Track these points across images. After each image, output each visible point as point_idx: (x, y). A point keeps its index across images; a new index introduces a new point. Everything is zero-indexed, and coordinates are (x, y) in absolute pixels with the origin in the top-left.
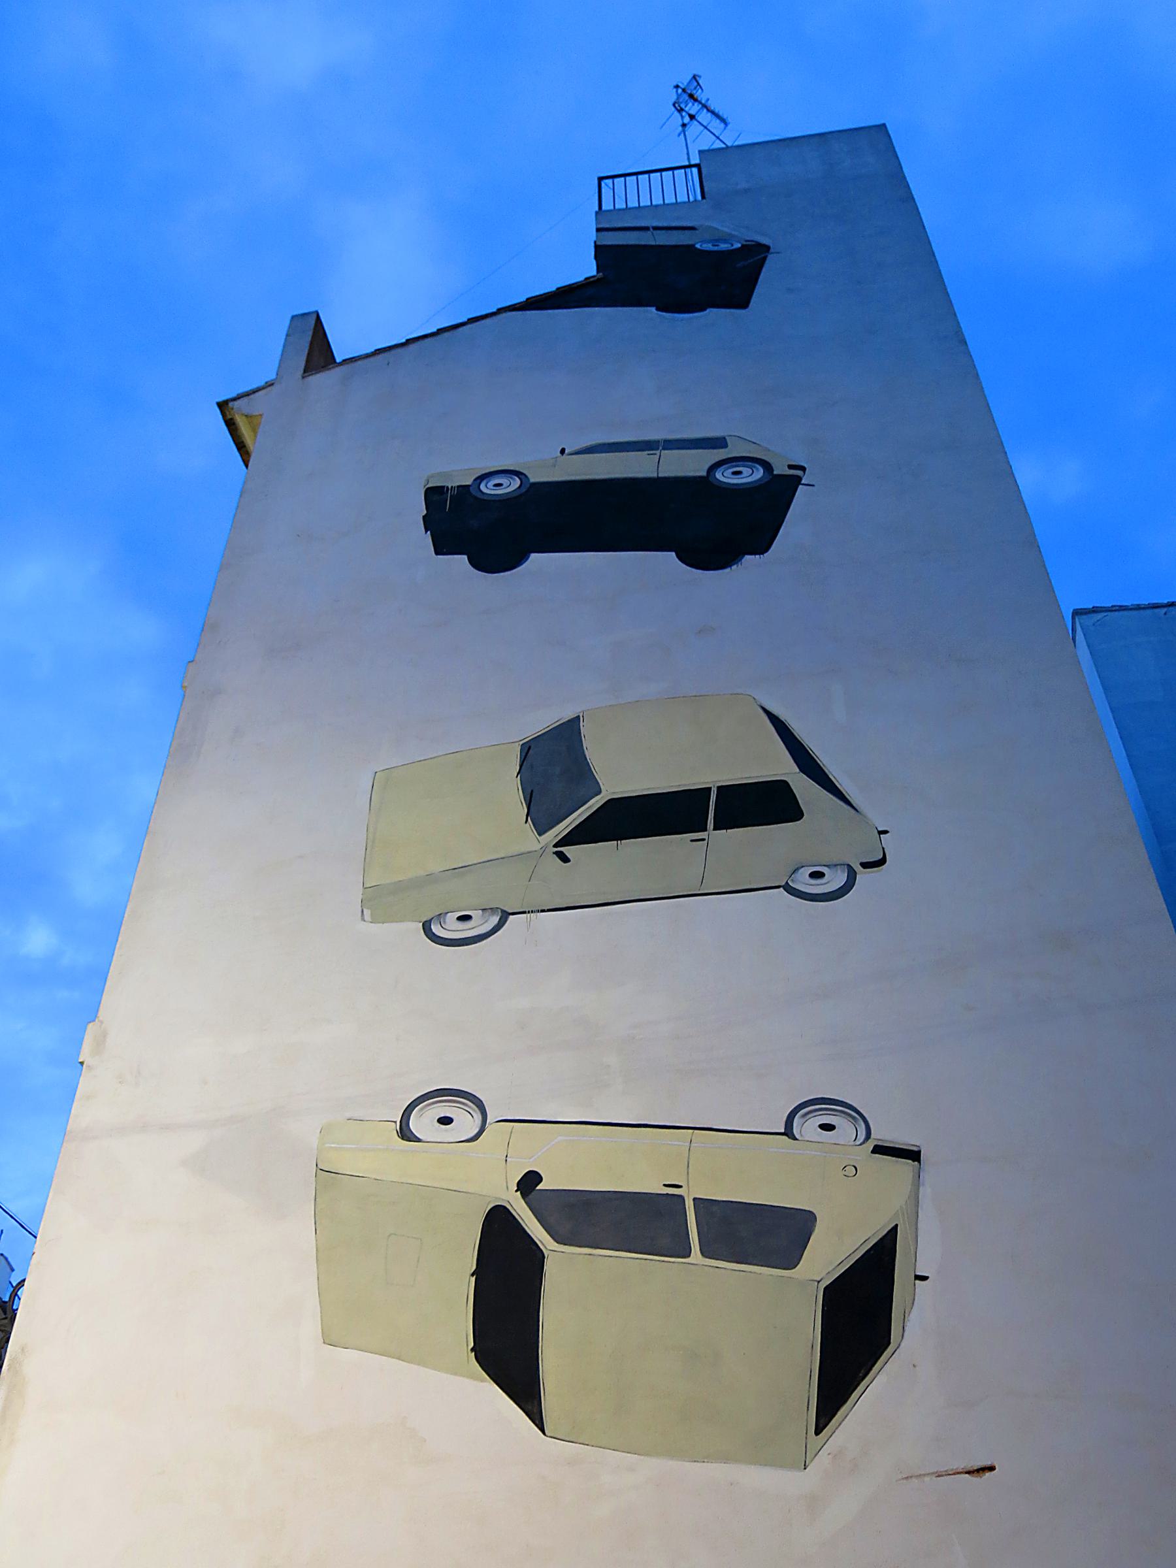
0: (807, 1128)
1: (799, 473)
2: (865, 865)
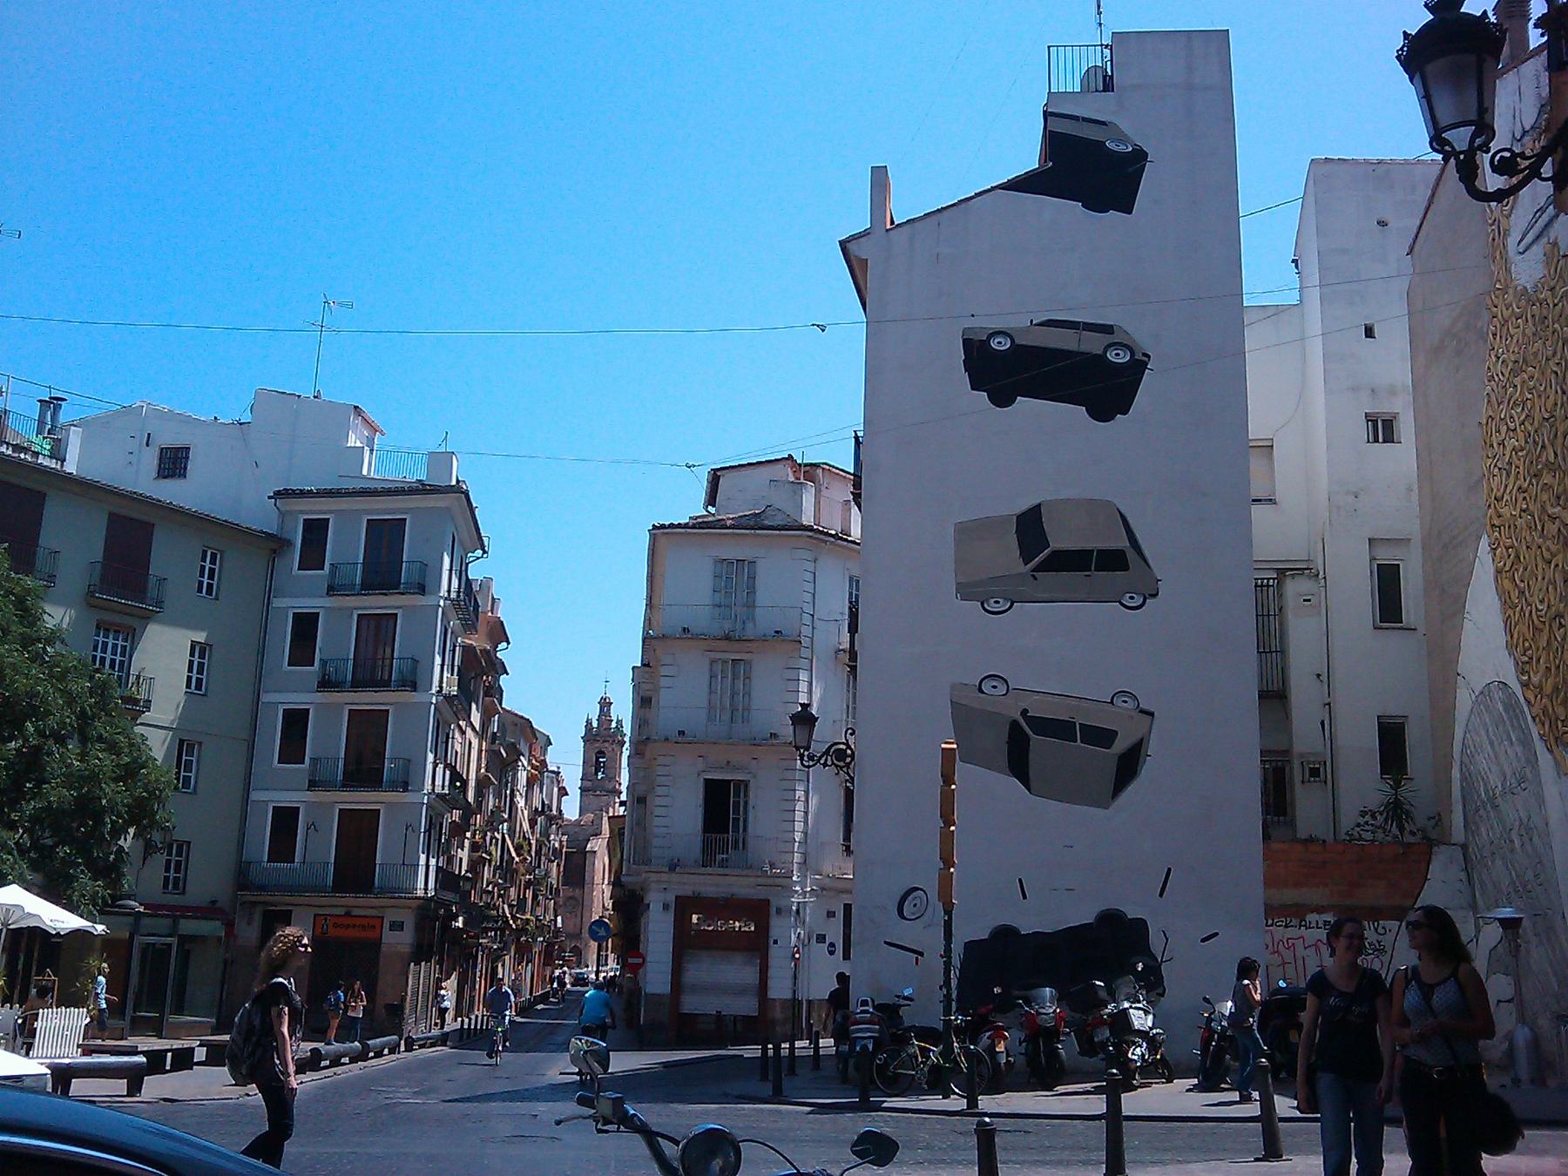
2: (1150, 595)
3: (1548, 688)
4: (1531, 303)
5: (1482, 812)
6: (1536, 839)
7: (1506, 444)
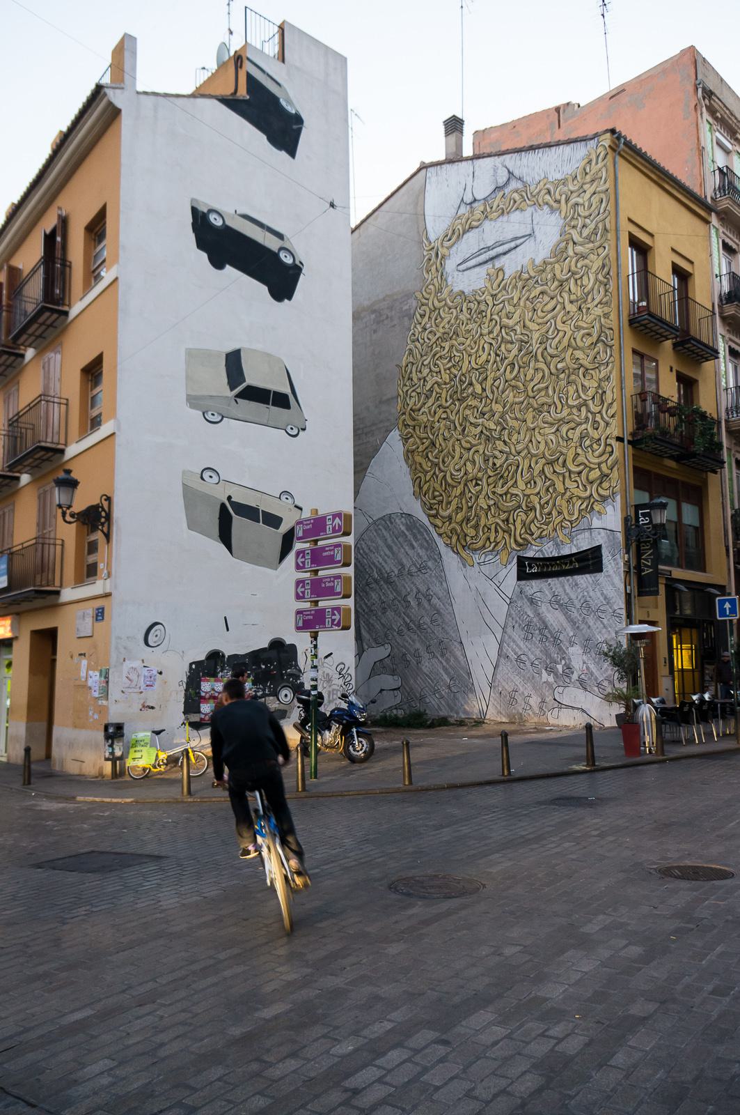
0: (283, 497)
3: (460, 517)
4: (467, 301)
5: (373, 585)
6: (435, 601)
7: (427, 379)
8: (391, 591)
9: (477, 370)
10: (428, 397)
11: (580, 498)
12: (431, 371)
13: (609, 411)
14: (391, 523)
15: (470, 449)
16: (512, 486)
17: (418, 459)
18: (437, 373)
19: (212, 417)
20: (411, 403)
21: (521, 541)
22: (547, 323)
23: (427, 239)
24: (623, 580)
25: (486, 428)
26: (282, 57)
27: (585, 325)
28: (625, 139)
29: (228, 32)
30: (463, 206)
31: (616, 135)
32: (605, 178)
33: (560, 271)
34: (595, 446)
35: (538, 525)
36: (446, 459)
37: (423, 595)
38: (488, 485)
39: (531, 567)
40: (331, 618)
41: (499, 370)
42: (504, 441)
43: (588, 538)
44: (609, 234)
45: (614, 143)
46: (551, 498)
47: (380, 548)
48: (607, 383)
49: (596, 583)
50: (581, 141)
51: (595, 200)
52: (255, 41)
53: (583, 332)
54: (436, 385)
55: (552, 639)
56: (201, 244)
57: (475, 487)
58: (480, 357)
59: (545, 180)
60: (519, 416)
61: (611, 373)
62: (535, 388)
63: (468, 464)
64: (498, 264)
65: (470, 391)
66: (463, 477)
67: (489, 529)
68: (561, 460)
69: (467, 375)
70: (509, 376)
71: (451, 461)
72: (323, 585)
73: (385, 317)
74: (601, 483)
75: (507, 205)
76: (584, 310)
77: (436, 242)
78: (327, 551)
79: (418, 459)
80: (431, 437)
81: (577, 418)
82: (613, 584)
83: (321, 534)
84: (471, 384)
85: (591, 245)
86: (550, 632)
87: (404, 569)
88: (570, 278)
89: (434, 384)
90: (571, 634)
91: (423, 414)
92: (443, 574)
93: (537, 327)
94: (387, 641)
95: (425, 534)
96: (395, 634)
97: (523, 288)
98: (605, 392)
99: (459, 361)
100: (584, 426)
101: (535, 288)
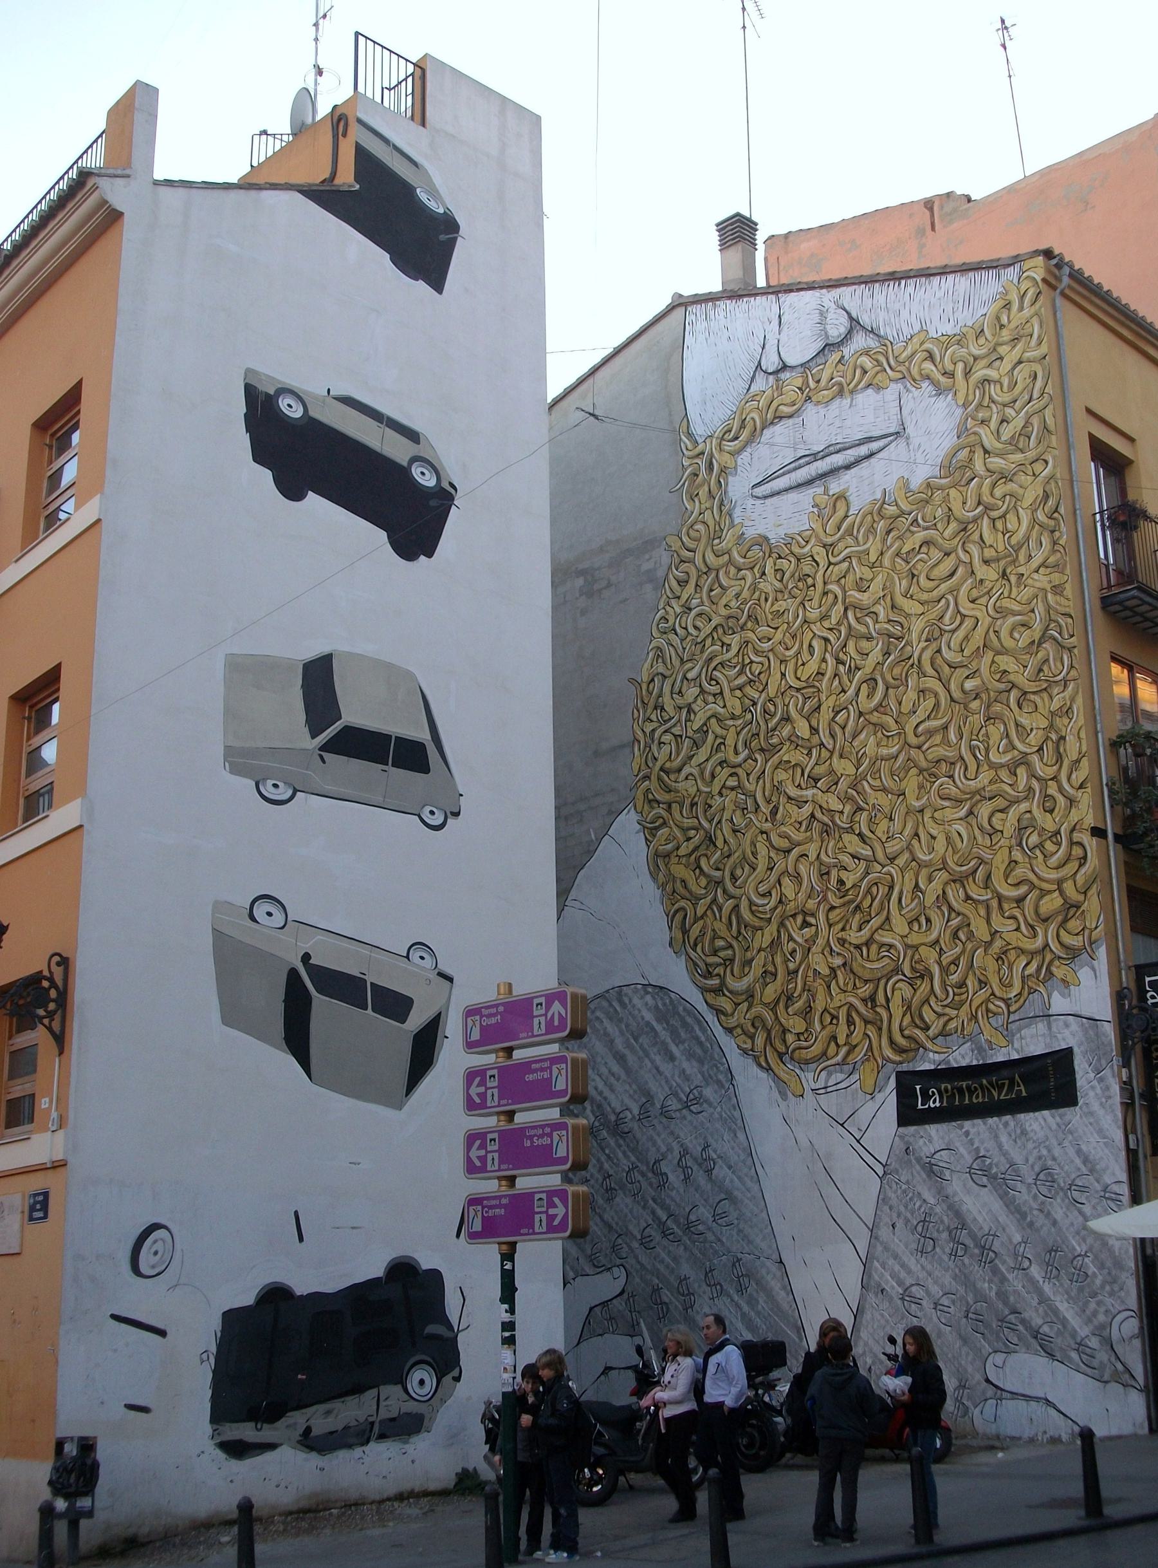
0: (415, 956)
1: (453, 491)
3: (770, 992)
6: (721, 1171)
7: (695, 707)
8: (624, 1153)
9: (798, 690)
10: (696, 745)
11: (1023, 951)
12: (702, 691)
13: (1074, 776)
14: (623, 1005)
15: (789, 851)
16: (880, 928)
17: (679, 871)
18: (714, 695)
19: (272, 789)
20: (662, 755)
21: (902, 1042)
22: (939, 601)
23: (690, 435)
24: (1121, 1123)
25: (821, 807)
26: (420, 115)
27: (1016, 607)
28: (1071, 267)
29: (313, 72)
30: (760, 377)
31: (1054, 262)
32: (1039, 337)
33: (962, 504)
34: (1049, 846)
35: (938, 1009)
36: (739, 872)
37: (695, 1160)
38: (830, 926)
39: (926, 1097)
40: (546, 1212)
41: (844, 691)
42: (860, 835)
43: (1044, 1035)
44: (1054, 438)
45: (1049, 271)
46: (963, 952)
47: (599, 1059)
48: (1066, 721)
49: (1065, 1129)
50: (988, 268)
51: (1021, 374)
52: (371, 89)
53: (1012, 620)
54: (713, 721)
55: (977, 1251)
56: (261, 455)
57: (801, 929)
58: (803, 664)
59: (922, 336)
60: (888, 783)
61: (1073, 700)
62: (920, 729)
63: (786, 881)
64: (835, 487)
65: (785, 732)
66: (775, 908)
67: (833, 1017)
68: (980, 874)
69: (779, 701)
70: (865, 704)
71: (749, 876)
72: (528, 1143)
73: (604, 583)
74: (1066, 920)
75: (849, 377)
76: (1013, 579)
77: (708, 441)
78: (536, 1071)
79: (679, 871)
80: (705, 824)
81: (1008, 789)
82: (1100, 1132)
83: (522, 1035)
84: (787, 719)
85: (1019, 457)
86: (973, 1236)
87: (653, 1104)
88: (981, 516)
89: (709, 718)
90: (1017, 1238)
91: (686, 778)
92: (737, 1114)
93: (920, 609)
94: (618, 1262)
95: (696, 1028)
96: (635, 1245)
97: (888, 532)
98: (1063, 738)
99: (760, 673)
100: (1024, 806)
101: (913, 533)
